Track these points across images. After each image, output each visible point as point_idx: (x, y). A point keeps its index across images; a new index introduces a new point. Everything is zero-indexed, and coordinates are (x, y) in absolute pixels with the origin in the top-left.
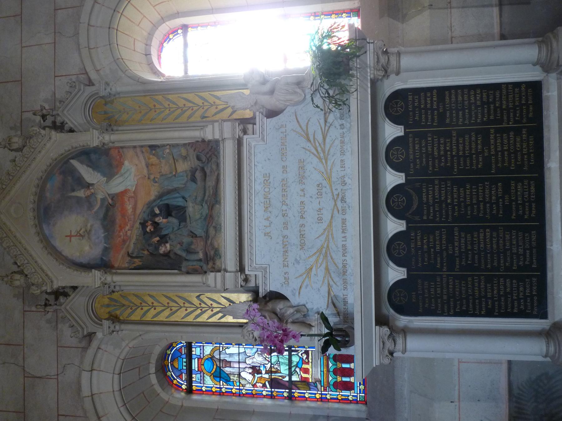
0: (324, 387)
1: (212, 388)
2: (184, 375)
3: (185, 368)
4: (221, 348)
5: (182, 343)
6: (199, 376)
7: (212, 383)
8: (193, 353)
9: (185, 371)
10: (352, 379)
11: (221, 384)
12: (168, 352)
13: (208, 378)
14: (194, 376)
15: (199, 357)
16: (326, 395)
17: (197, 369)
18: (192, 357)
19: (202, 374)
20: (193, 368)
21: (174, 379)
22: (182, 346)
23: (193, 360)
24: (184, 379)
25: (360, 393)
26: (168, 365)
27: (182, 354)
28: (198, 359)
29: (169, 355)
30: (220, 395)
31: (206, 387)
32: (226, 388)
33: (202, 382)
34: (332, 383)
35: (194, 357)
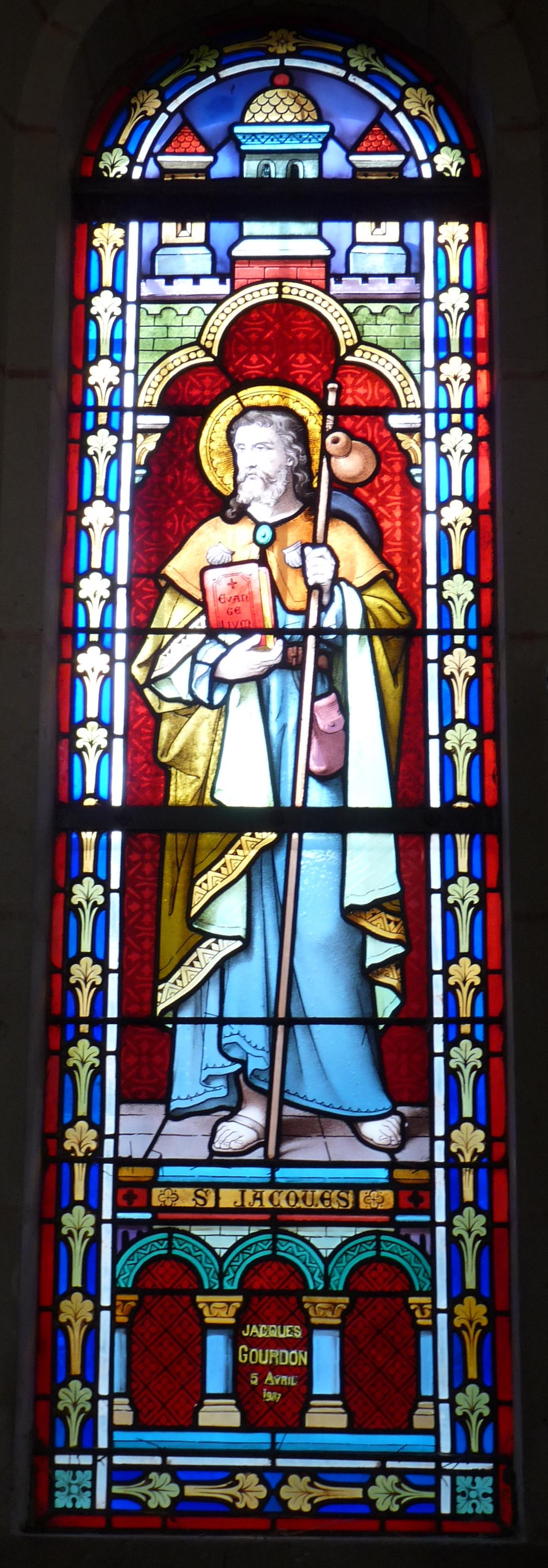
2: (201, 160)
3: (251, 168)
4: (414, 420)
5: (430, 157)
10: (220, 1414)
11: (145, 421)
14: (197, 230)
15: (337, 265)
16: (93, 1206)
20: (250, 227)
23: (311, 228)
25: (117, 1475)
27: (350, 150)
28: (326, 260)
35: (338, 231)
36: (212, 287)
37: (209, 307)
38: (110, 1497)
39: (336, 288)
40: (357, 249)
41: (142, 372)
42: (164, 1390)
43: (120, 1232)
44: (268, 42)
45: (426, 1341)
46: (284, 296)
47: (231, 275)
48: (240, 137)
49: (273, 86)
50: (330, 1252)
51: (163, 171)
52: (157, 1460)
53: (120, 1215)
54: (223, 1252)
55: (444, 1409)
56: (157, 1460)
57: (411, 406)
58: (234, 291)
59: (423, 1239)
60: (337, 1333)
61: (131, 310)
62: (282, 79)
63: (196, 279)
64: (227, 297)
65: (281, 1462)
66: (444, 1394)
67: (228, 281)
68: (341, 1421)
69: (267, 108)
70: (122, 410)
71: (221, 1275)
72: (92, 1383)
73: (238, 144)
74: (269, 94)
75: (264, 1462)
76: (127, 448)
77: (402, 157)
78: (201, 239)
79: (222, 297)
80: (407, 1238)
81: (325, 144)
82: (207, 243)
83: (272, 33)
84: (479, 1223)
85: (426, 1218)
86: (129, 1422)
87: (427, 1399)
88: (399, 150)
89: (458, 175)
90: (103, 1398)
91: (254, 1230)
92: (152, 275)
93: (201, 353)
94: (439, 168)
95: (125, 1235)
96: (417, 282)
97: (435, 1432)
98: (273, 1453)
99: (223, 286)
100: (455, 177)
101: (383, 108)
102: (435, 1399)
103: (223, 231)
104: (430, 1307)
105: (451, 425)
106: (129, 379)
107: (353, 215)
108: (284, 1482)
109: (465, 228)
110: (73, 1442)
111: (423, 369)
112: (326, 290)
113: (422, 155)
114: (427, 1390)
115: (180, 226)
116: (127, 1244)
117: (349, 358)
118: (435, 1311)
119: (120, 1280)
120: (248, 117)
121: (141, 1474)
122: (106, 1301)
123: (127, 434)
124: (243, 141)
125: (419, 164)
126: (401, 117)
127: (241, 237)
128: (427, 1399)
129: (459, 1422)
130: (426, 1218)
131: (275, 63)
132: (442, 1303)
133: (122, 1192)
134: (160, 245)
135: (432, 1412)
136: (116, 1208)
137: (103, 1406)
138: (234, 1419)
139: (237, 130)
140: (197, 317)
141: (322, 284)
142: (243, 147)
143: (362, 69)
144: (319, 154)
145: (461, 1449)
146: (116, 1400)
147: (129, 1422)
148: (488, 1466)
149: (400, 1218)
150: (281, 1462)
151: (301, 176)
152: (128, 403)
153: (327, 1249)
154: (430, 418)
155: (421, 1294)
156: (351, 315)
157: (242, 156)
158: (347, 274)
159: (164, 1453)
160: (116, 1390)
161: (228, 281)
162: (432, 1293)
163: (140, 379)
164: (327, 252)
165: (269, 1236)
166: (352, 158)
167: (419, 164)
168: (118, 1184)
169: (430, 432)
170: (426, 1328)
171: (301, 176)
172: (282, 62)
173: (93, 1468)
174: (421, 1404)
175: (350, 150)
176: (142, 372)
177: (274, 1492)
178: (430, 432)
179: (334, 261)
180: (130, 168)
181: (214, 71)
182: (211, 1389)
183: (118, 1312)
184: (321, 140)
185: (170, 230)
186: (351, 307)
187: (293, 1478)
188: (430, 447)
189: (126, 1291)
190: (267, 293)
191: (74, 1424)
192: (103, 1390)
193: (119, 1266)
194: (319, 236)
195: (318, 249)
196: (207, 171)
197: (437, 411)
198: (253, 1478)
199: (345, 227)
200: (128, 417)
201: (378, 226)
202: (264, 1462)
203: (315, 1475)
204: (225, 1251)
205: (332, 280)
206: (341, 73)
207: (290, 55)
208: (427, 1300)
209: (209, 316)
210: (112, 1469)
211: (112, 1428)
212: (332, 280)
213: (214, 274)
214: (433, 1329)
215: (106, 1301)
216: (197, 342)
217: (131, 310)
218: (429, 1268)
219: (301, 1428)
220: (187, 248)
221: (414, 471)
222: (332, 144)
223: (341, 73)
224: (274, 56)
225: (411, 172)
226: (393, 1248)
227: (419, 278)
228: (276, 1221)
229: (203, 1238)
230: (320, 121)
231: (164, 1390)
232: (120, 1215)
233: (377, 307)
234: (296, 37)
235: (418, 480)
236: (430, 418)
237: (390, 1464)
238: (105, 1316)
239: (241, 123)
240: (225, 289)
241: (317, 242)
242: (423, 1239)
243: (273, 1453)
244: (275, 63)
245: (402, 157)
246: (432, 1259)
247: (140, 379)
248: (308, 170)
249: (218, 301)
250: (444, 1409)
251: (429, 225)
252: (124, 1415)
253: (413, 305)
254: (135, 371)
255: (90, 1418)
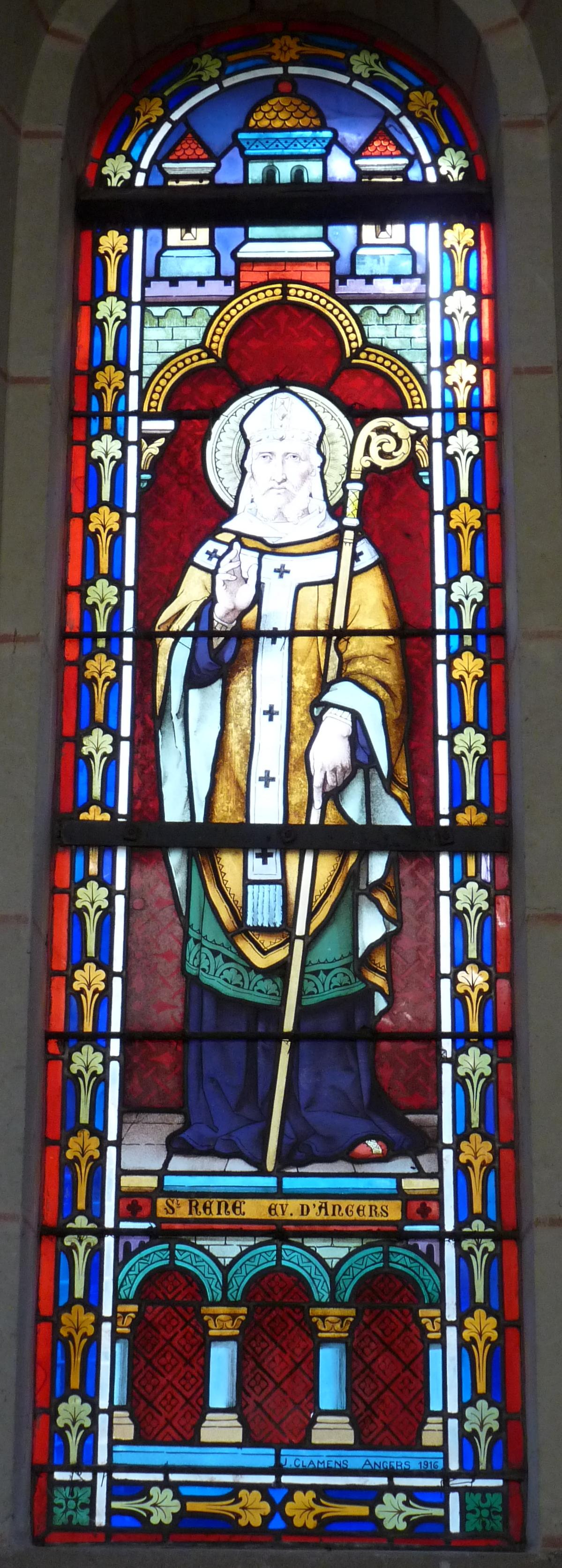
0: (151, 1195)
1: (121, 363)
6: (204, 265)
7: (152, 360)
8: (369, 231)
9: (230, 175)
10: (222, 1428)
12: (361, 63)
13: (193, 335)
14: (202, 235)
15: (342, 266)
17: (249, 251)
18: (342, 220)
19: (216, 289)
20: (255, 232)
21: (169, 107)
22: (414, 157)
23: (316, 231)
24: (170, 167)
26: (270, 62)
28: (331, 262)
29: (345, 69)
30: (73, 415)
31: (125, 323)
32: (121, 464)
33: (158, 289)
34: (186, 1256)
35: (343, 235)
36: (216, 289)
37: (212, 310)
38: (110, 1513)
39: (340, 290)
40: (361, 252)
41: (147, 372)
42: (166, 1405)
43: (122, 1241)
44: (272, 50)
45: (435, 1354)
46: (290, 298)
47: (237, 278)
48: (244, 144)
49: (276, 93)
50: (335, 1262)
51: (167, 177)
52: (159, 1477)
53: (124, 1225)
54: (228, 1261)
55: (453, 1424)
56: (159, 1477)
57: (418, 407)
58: (239, 291)
59: (430, 1248)
60: (343, 1346)
61: (136, 311)
62: (285, 87)
63: (201, 281)
64: (231, 298)
65: (285, 1479)
66: (453, 1408)
67: (233, 283)
68: (348, 1436)
69: (273, 114)
70: (126, 414)
71: (225, 1288)
72: (92, 1399)
73: (242, 150)
74: (272, 102)
75: (270, 1479)
76: (132, 451)
77: (405, 161)
78: (206, 242)
79: (225, 299)
80: (415, 1249)
81: (328, 149)
82: (211, 246)
83: (275, 41)
84: (484, 1151)
85: (435, 1228)
86: (130, 1437)
87: (435, 1414)
88: (404, 154)
89: (461, 178)
90: (104, 1411)
91: (259, 1240)
92: (157, 277)
93: (204, 355)
94: (443, 171)
95: (127, 1246)
96: (422, 283)
97: (443, 1448)
98: (278, 1470)
99: (228, 287)
100: (458, 181)
101: (387, 113)
102: (444, 1414)
103: (230, 235)
104: (439, 1319)
105: (458, 427)
106: (134, 381)
107: (357, 218)
108: (289, 1497)
109: (470, 233)
110: (73, 1458)
111: (429, 369)
112: (331, 292)
113: (426, 158)
114: (435, 1405)
115: (184, 231)
116: (129, 1254)
117: (354, 361)
118: (445, 1324)
119: (121, 1292)
120: (252, 123)
121: (141, 1490)
122: (107, 1311)
123: (133, 436)
124: (247, 146)
125: (423, 167)
126: (405, 121)
127: (247, 240)
128: (435, 1414)
129: (467, 1439)
130: (435, 1228)
131: (279, 71)
132: (451, 1314)
133: (124, 1203)
134: (165, 247)
135: (441, 1427)
136: (118, 1218)
137: (103, 1419)
138: (237, 1435)
139: (242, 136)
140: (201, 318)
141: (327, 287)
142: (248, 152)
143: (366, 75)
144: (323, 158)
145: (469, 1466)
146: (116, 1413)
147: (130, 1437)
148: (499, 1483)
149: (408, 1228)
150: (285, 1479)
151: (306, 181)
152: (133, 406)
153: (332, 1259)
154: (437, 418)
155: (431, 1306)
156: (356, 317)
157: (247, 160)
158: (353, 275)
159: (167, 1470)
160: (116, 1403)
161: (233, 283)
162: (441, 1305)
163: (145, 381)
164: (331, 254)
165: (274, 1247)
166: (357, 162)
167: (423, 167)
168: (120, 1194)
169: (437, 433)
170: (434, 1341)
171: (306, 181)
172: (285, 70)
173: (93, 1484)
174: (429, 1419)
175: (354, 156)
176: (147, 372)
177: (278, 1509)
178: (437, 433)
179: (338, 263)
180: (133, 173)
181: (218, 81)
182: (214, 1403)
183: (120, 1323)
184: (325, 144)
185: (174, 235)
186: (357, 308)
187: (298, 1495)
188: (437, 447)
189: (127, 1301)
190: (273, 294)
191: (74, 1441)
192: (104, 1403)
193: (121, 1277)
194: (325, 239)
195: (321, 250)
196: (211, 176)
197: (444, 410)
198: (256, 1494)
199: (350, 230)
200: (133, 421)
201: (383, 229)
202: (270, 1479)
203: (323, 1492)
204: (230, 1260)
205: (337, 281)
206: (345, 79)
207: (294, 63)
208: (436, 1312)
209: (213, 318)
210: (112, 1485)
211: (112, 1443)
212: (337, 281)
213: (218, 276)
214: (442, 1342)
215: (107, 1311)
216: (202, 345)
217: (136, 311)
218: (438, 1282)
219: (305, 1443)
220: (189, 252)
221: (421, 474)
222: (335, 149)
223: (345, 79)
224: (278, 63)
225: (414, 174)
226: (402, 1259)
227: (425, 279)
228: (279, 1233)
229: (206, 1247)
230: (323, 127)
231: (166, 1405)
232: (124, 1225)
233: (383, 309)
234: (299, 44)
235: (426, 481)
236: (437, 418)
237: (398, 1481)
238: (106, 1327)
239: (247, 129)
240: (230, 290)
241: (322, 246)
242: (430, 1248)
243: (278, 1470)
244: (279, 71)
245: (405, 161)
246: (440, 1270)
247: (145, 381)
248: (313, 172)
249: (222, 303)
250: (453, 1424)
251: (435, 227)
252: (126, 1430)
253: (418, 306)
254: (139, 373)
255: (91, 1433)
